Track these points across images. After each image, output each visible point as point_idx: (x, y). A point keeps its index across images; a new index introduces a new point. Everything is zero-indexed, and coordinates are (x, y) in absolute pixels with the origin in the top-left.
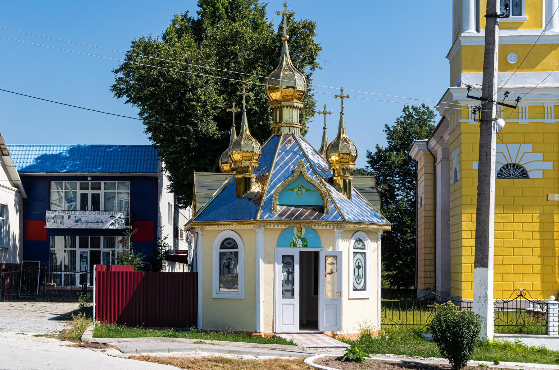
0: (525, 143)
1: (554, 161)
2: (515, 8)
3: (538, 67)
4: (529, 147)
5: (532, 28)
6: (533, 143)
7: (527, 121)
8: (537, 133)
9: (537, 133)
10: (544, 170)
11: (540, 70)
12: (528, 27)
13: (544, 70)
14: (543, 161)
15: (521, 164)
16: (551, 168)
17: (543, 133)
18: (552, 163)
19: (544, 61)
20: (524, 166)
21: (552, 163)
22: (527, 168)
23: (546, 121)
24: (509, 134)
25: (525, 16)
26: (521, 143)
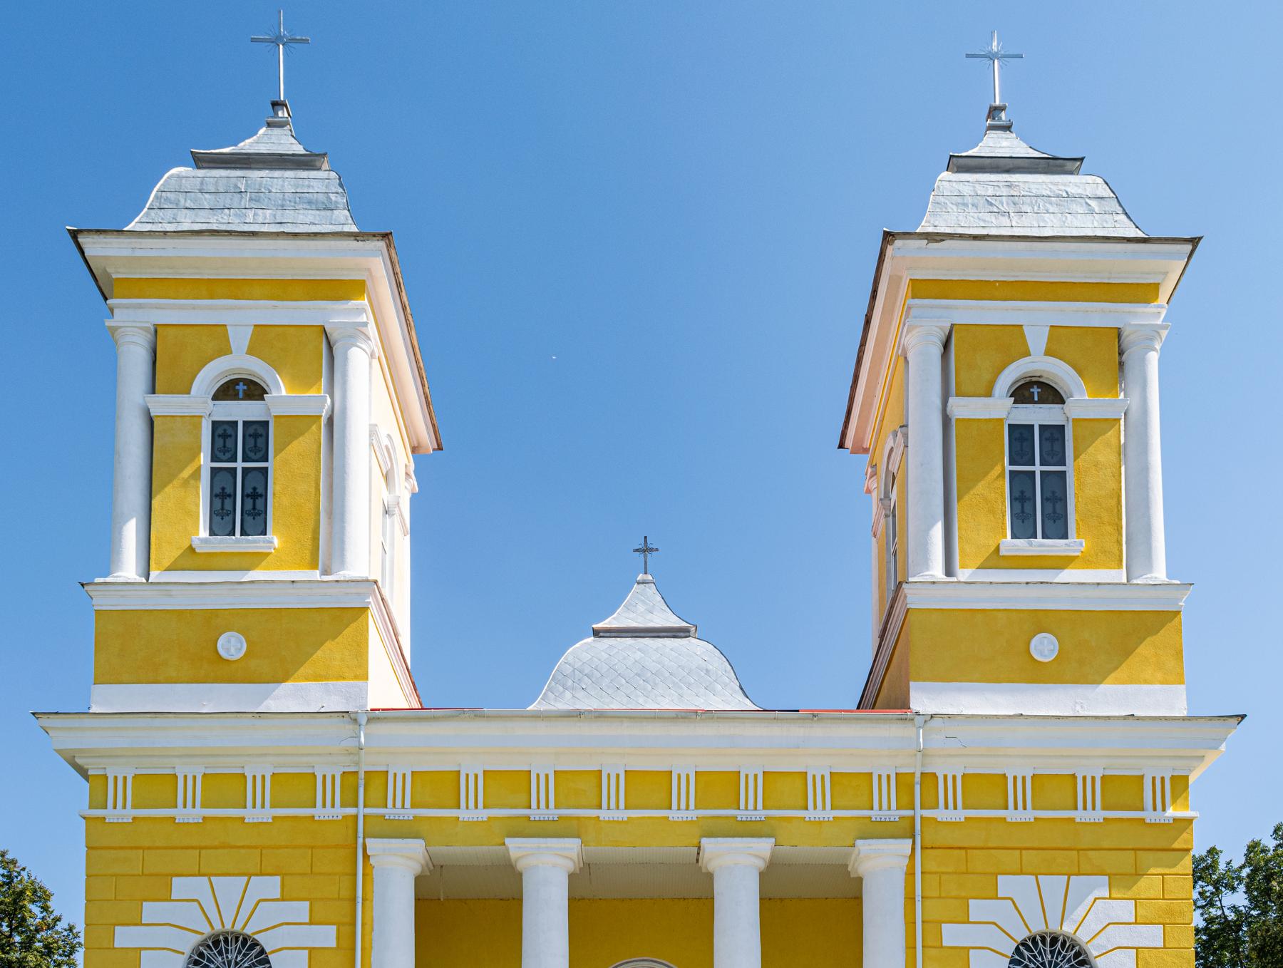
0: (261, 874)
1: (339, 925)
2: (249, 519)
3: (302, 671)
4: (271, 886)
5: (290, 568)
6: (283, 876)
7: (266, 814)
8: (295, 847)
9: (295, 847)
10: (311, 950)
11: (307, 680)
12: (279, 566)
13: (317, 677)
14: (311, 923)
15: (248, 931)
16: (334, 945)
17: (312, 848)
18: (334, 928)
19: (319, 653)
20: (256, 937)
21: (334, 928)
22: (267, 942)
23: (319, 812)
24: (220, 851)
25: (274, 540)
26: (250, 875)
